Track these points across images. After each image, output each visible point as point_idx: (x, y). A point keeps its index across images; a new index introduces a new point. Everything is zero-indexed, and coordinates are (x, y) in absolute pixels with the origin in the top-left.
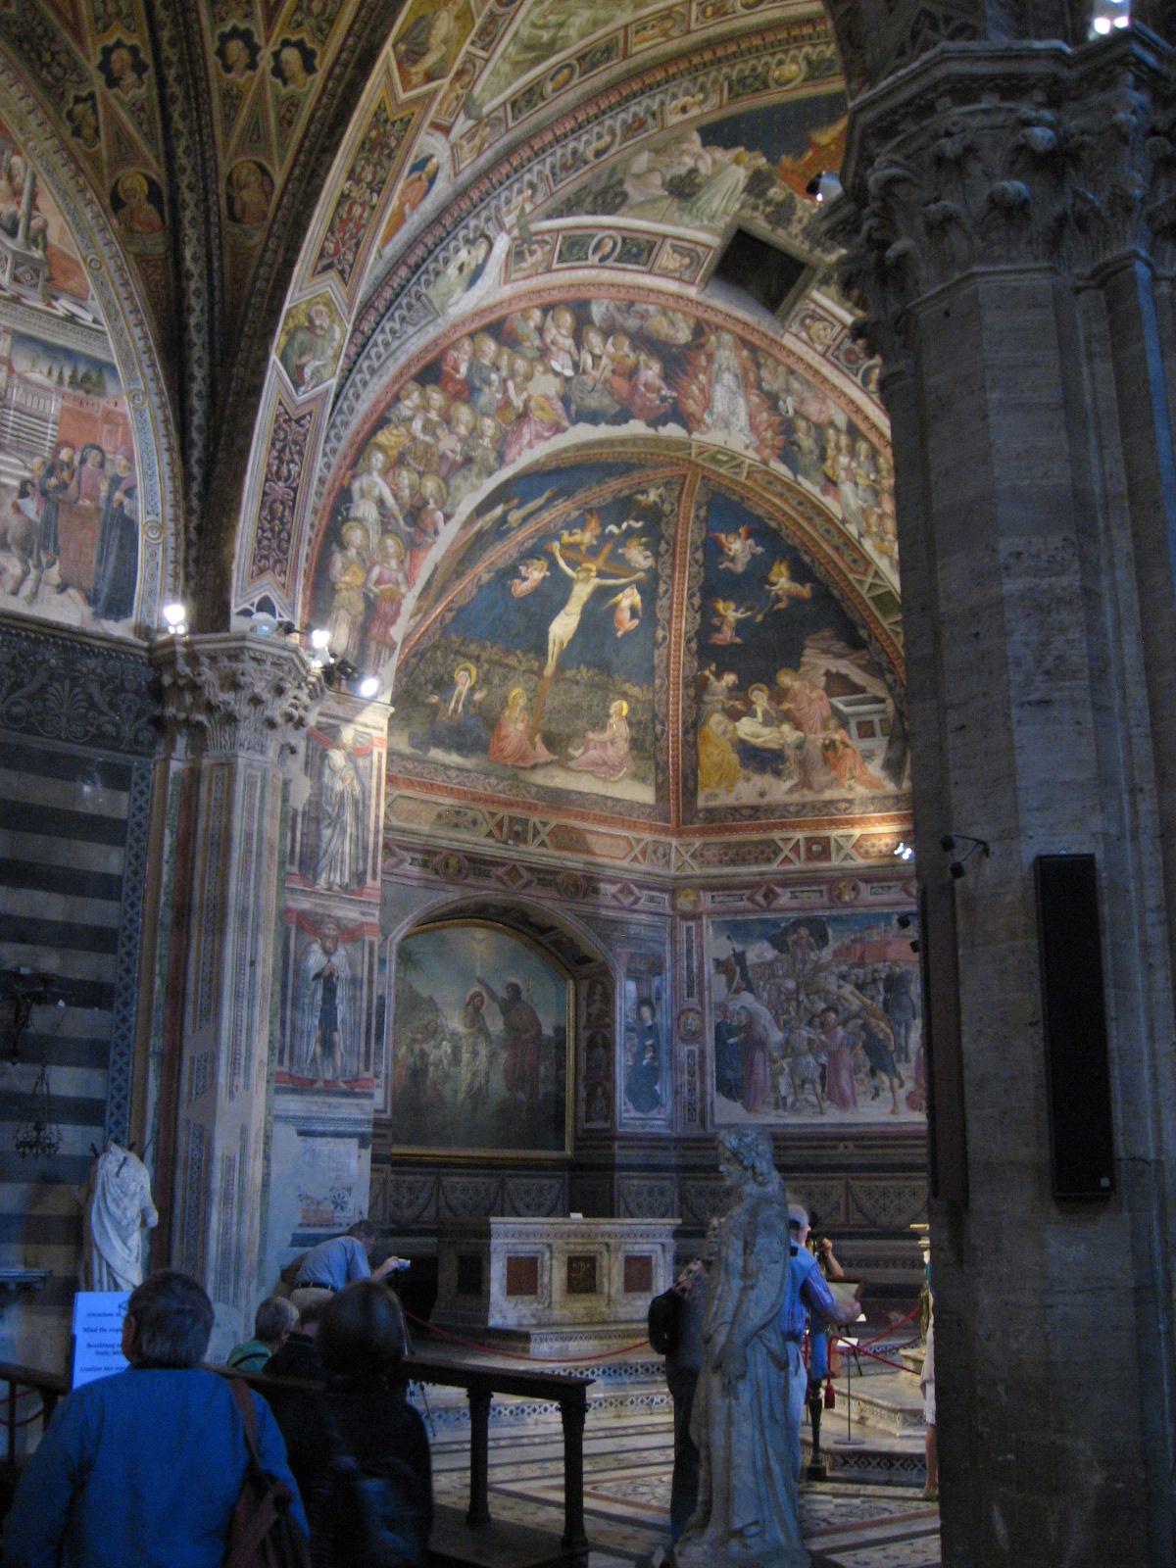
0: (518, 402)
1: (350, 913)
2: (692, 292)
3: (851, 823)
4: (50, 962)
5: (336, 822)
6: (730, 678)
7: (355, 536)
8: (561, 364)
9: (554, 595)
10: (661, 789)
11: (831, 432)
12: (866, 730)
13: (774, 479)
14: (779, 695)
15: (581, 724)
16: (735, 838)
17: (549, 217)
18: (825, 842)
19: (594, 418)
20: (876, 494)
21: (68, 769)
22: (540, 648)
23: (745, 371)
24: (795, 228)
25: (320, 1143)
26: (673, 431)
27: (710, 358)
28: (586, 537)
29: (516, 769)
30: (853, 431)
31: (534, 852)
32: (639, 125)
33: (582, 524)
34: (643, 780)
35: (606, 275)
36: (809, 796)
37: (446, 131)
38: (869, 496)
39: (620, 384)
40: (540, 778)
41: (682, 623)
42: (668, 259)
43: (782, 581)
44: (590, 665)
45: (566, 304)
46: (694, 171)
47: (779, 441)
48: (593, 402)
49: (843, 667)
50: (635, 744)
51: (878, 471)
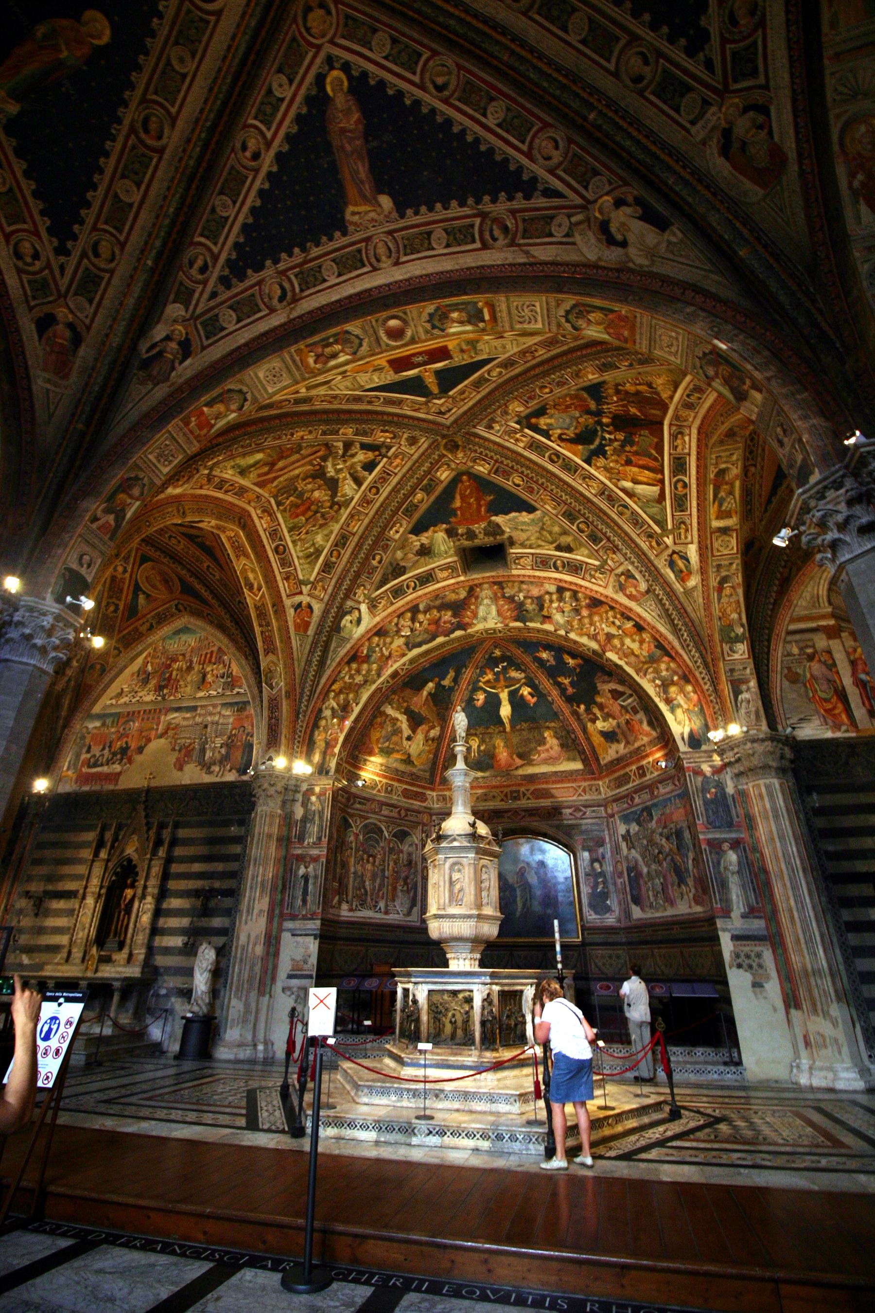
0: (386, 653)
1: (315, 852)
2: (462, 578)
3: (647, 756)
4: (217, 884)
5: (312, 821)
6: (582, 707)
7: (323, 723)
8: (406, 632)
9: (494, 702)
10: (585, 761)
11: (547, 597)
12: (636, 712)
13: (519, 629)
14: (601, 707)
15: (533, 745)
16: (616, 775)
17: (378, 589)
18: (642, 767)
19: (419, 645)
20: (577, 611)
21: (227, 823)
22: (499, 721)
23: (495, 594)
24: (481, 536)
25: (299, 939)
26: (458, 633)
27: (477, 598)
28: (490, 676)
29: (507, 772)
30: (561, 590)
31: (523, 803)
32: (386, 548)
33: (483, 673)
34: (574, 759)
35: (420, 593)
36: (632, 748)
37: (301, 593)
38: (573, 614)
39: (433, 628)
40: (520, 772)
41: (555, 693)
42: (441, 575)
43: (571, 662)
44: (526, 721)
45: (409, 610)
46: (422, 545)
47: (515, 614)
48: (419, 640)
49: (613, 686)
50: (562, 746)
51: (577, 600)
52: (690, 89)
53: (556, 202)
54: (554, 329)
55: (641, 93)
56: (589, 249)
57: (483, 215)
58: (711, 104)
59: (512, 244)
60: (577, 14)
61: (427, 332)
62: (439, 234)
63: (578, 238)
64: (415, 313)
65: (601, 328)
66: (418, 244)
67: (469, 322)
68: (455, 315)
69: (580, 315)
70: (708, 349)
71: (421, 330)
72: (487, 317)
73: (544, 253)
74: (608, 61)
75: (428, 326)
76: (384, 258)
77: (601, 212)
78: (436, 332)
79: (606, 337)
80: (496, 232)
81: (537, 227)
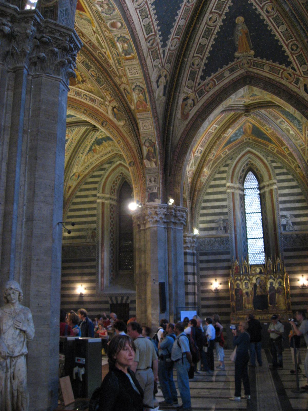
52: (193, 81)
53: (162, 56)
54: (130, 81)
55: (190, 66)
56: (153, 76)
57: (155, 35)
58: (192, 89)
59: (149, 49)
60: (206, 40)
61: (115, 36)
62: (147, 20)
63: (155, 70)
64: (124, 32)
65: (138, 99)
66: (144, 14)
67: (123, 50)
68: (126, 45)
69: (140, 91)
70: (154, 142)
71: (116, 33)
72: (127, 57)
73: (149, 62)
74: (196, 53)
75: (119, 36)
76: (137, 3)
77: (163, 72)
78: (116, 39)
79: (136, 101)
80: (151, 42)
81: (155, 56)
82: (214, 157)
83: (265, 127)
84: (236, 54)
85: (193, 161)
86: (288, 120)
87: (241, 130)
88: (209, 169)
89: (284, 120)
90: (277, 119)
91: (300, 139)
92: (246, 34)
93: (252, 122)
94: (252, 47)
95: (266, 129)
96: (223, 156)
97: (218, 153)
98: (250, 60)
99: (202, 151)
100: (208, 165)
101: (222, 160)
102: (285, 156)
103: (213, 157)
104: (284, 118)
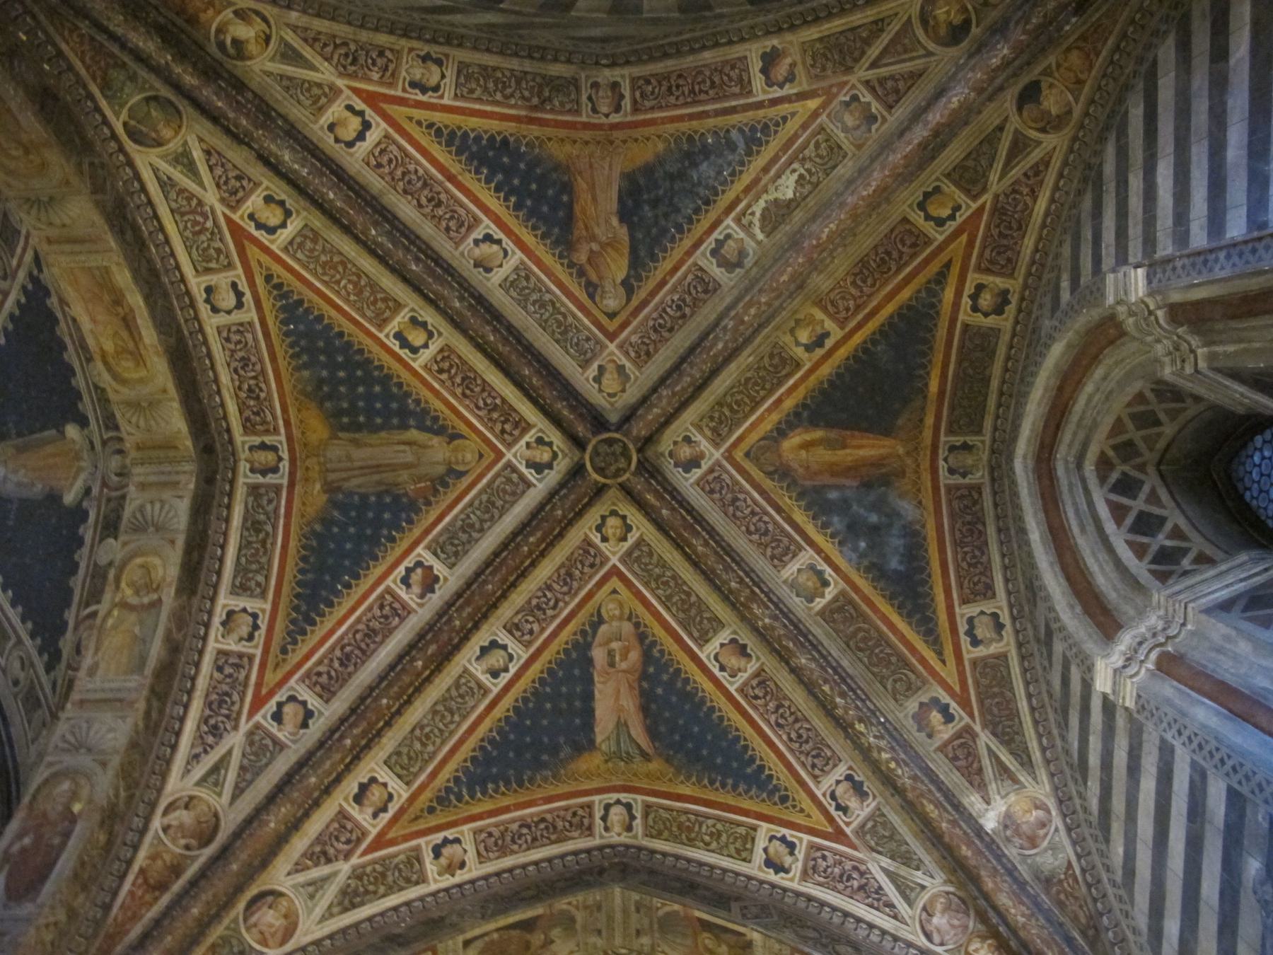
82: (954, 707)
83: (799, 352)
84: (69, 498)
85: (886, 862)
86: (705, 224)
87: (833, 495)
88: (1023, 777)
89: (710, 243)
90: (708, 287)
91: (822, 129)
92: (20, 450)
93: (767, 426)
94: (54, 432)
95: (809, 348)
96: (1007, 644)
97: (949, 672)
98: (104, 443)
99: (849, 778)
100: (989, 771)
101: (1023, 658)
102: (998, 211)
103: (949, 718)
104: (687, 243)
